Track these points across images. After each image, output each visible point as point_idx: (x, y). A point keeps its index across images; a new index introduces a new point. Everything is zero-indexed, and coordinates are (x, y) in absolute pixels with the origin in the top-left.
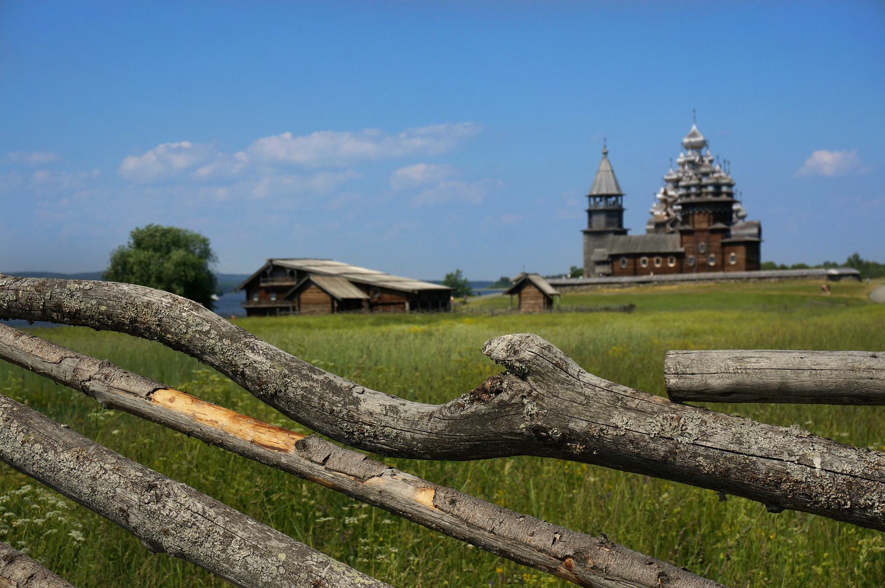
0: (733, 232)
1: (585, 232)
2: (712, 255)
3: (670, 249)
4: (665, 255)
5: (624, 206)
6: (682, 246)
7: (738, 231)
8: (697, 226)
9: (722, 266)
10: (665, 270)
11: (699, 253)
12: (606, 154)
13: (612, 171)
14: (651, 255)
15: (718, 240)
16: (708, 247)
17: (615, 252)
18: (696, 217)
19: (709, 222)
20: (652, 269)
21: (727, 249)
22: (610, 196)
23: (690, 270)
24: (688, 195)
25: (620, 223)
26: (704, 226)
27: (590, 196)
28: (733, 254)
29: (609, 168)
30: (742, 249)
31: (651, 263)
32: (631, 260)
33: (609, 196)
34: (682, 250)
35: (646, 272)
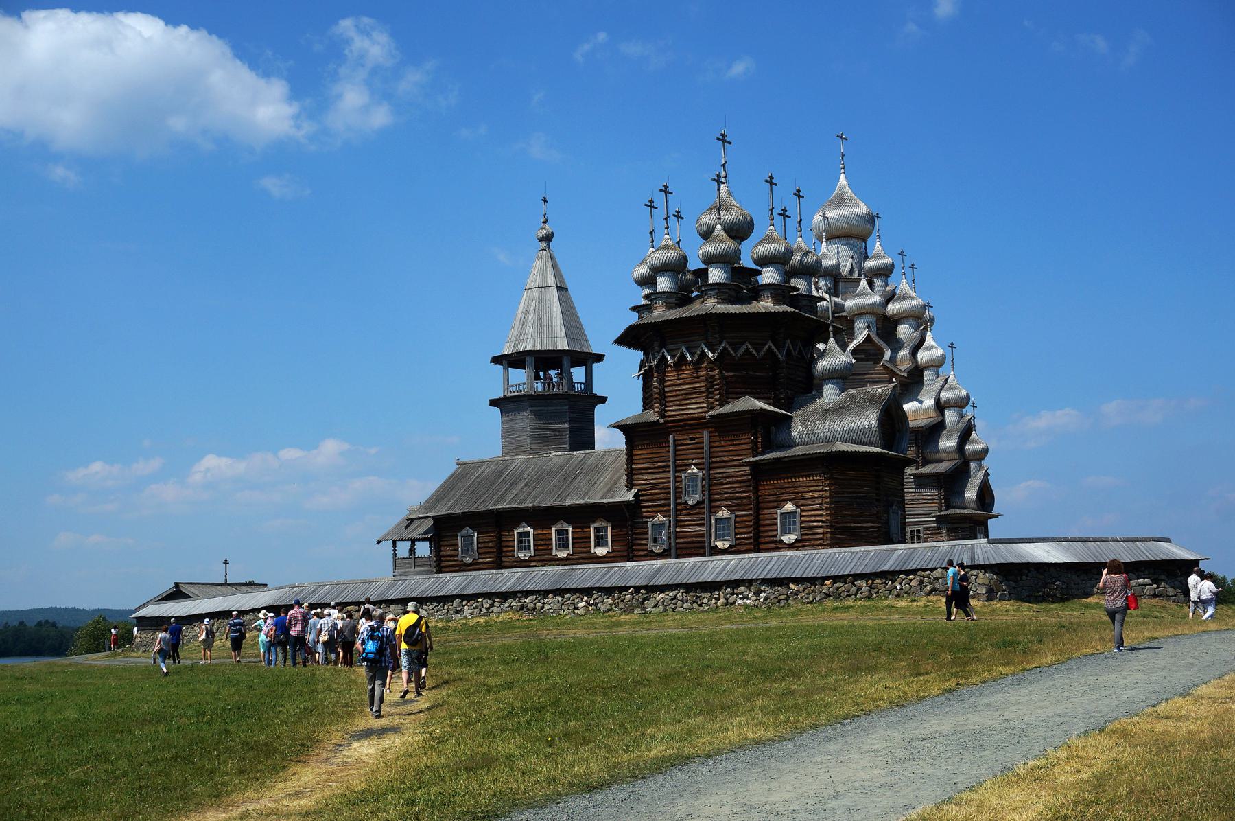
0: (797, 430)
2: (724, 513)
4: (582, 515)
5: (598, 390)
6: (630, 486)
8: (673, 410)
11: (681, 508)
12: (548, 238)
13: (562, 289)
14: (542, 517)
15: (742, 458)
16: (711, 484)
18: (671, 376)
19: (710, 394)
21: (769, 487)
22: (543, 361)
26: (696, 408)
28: (789, 507)
29: (551, 280)
30: (817, 487)
31: (543, 545)
32: (490, 537)
34: (629, 497)
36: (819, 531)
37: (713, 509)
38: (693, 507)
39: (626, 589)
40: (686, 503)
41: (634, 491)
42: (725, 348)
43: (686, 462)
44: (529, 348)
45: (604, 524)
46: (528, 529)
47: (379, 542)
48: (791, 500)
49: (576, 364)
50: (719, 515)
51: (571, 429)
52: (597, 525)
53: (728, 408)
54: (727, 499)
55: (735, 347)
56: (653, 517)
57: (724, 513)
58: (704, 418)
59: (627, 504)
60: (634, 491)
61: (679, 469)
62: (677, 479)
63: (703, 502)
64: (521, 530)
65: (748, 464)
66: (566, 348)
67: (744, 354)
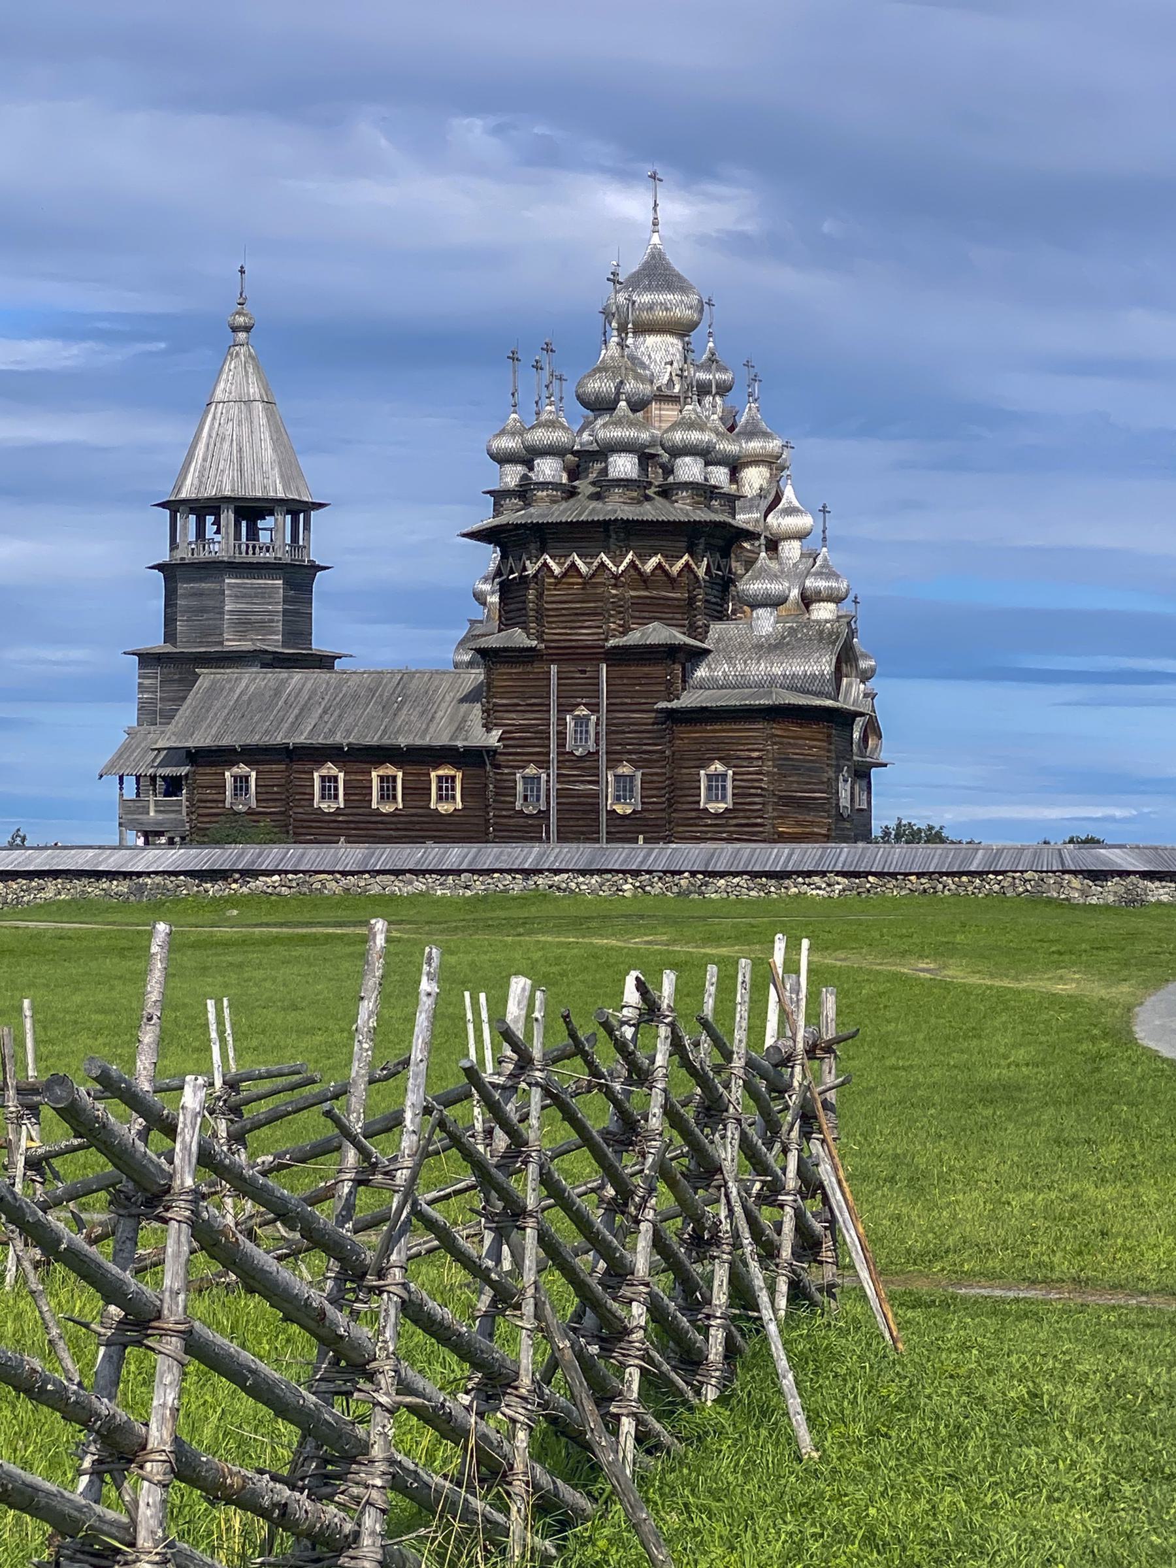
1: (147, 659)
3: (439, 735)
4: (419, 758)
7: (744, 661)
9: (668, 815)
10: (419, 826)
17: (201, 739)
20: (360, 825)
23: (528, 830)
24: (524, 492)
25: (298, 623)
27: (173, 506)
31: (358, 792)
33: (251, 511)
34: (493, 739)
35: (323, 830)
36: (757, 800)
37: (612, 764)
38: (581, 758)
39: (680, 873)
40: (572, 753)
41: (497, 733)
42: (632, 561)
43: (573, 701)
44: (227, 493)
45: (452, 773)
46: (334, 771)
47: (101, 776)
48: (719, 759)
49: (288, 512)
50: (620, 771)
51: (285, 611)
52: (440, 772)
53: (634, 637)
54: (630, 752)
55: (644, 558)
56: (524, 768)
57: (625, 769)
58: (603, 647)
59: (492, 752)
60: (497, 733)
61: (563, 710)
62: (562, 722)
63: (597, 752)
64: (324, 772)
65: (662, 710)
66: (281, 495)
67: (656, 568)
